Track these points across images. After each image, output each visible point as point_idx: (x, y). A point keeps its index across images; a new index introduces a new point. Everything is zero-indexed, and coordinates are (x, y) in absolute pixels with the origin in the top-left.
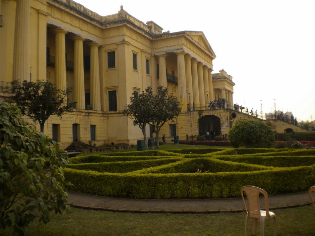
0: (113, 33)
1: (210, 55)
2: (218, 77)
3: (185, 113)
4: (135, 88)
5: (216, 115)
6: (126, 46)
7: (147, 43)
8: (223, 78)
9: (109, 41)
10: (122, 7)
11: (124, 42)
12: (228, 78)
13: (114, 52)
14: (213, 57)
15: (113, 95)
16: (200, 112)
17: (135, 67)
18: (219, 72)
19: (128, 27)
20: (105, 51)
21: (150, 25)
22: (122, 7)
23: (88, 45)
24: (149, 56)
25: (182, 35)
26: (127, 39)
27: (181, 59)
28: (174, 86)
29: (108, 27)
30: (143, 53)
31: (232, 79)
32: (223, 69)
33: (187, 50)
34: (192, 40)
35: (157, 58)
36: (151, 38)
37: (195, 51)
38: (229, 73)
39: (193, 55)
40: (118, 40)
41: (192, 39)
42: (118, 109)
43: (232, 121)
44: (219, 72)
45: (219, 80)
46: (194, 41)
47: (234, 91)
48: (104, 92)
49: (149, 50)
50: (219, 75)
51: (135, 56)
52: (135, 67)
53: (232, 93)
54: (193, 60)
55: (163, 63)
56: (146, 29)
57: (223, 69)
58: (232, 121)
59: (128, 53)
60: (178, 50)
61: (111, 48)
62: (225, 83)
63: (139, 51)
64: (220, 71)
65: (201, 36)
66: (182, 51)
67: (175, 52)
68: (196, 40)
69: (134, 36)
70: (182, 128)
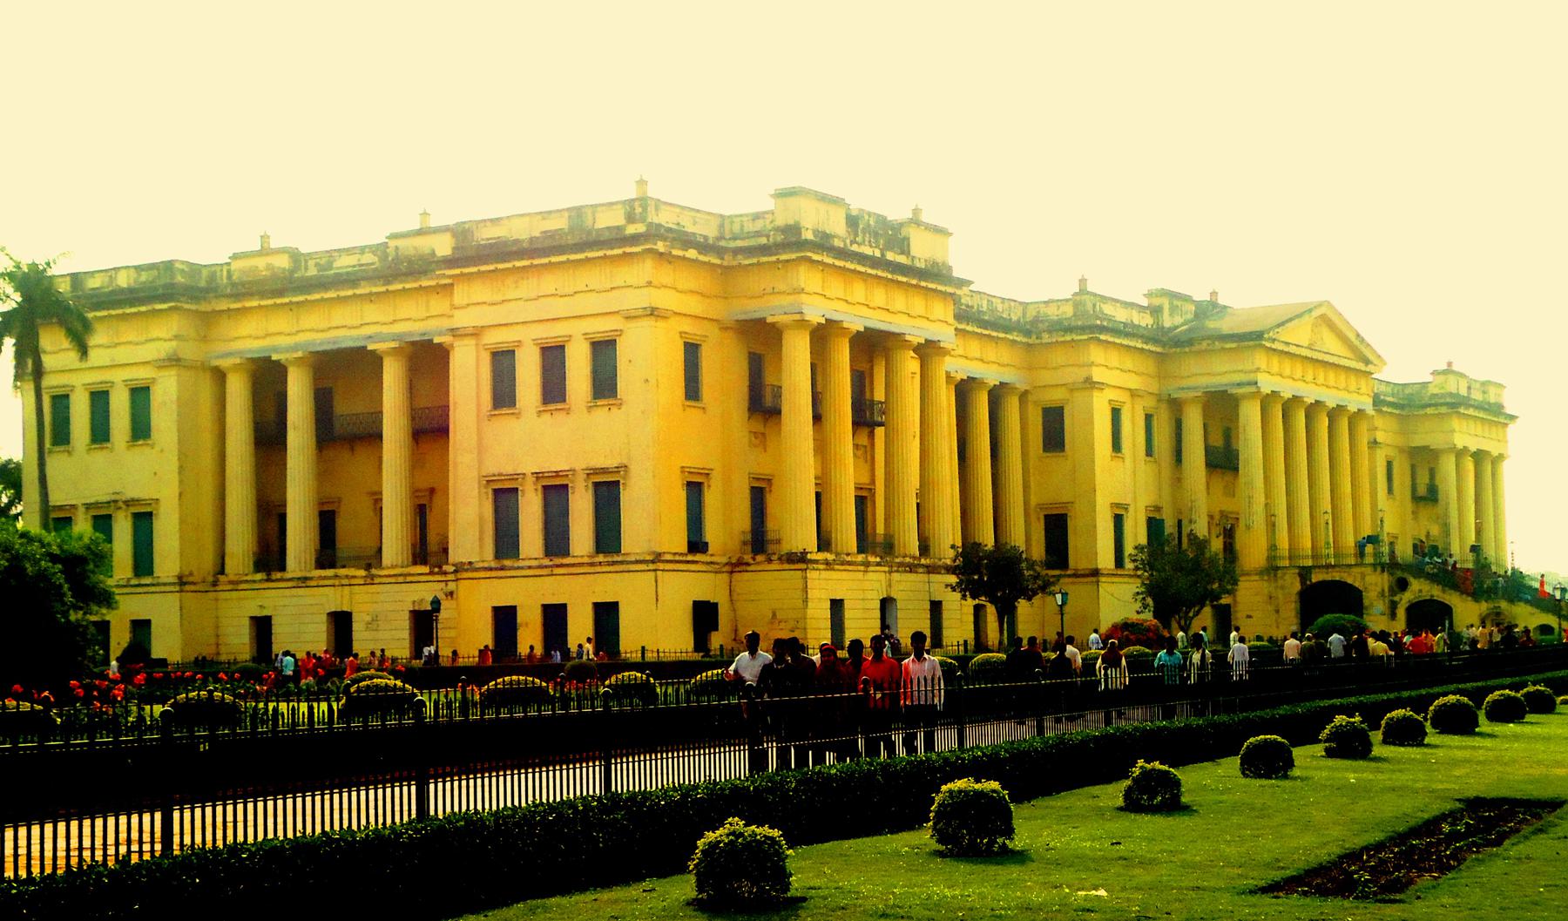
0: (1058, 357)
1: (1361, 359)
2: (1426, 400)
3: (1261, 573)
4: (1117, 505)
5: (1350, 581)
6: (1096, 394)
7: (1149, 366)
8: (1447, 404)
9: (1046, 377)
10: (1083, 281)
11: (1090, 384)
12: (1477, 396)
15: (1057, 527)
16: (1304, 573)
17: (1116, 445)
21: (1156, 302)
22: (1083, 281)
23: (997, 396)
26: (1098, 375)
27: (1250, 414)
28: (1229, 477)
29: (1046, 338)
33: (1267, 384)
34: (1286, 349)
36: (1159, 350)
40: (1076, 375)
41: (1287, 344)
42: (1072, 563)
43: (1396, 598)
44: (1429, 378)
45: (1429, 411)
46: (1293, 349)
48: (1033, 517)
50: (1433, 390)
51: (1116, 414)
53: (1501, 457)
56: (1146, 321)
58: (1396, 598)
61: (1055, 397)
62: (1456, 423)
66: (1253, 389)
68: (1298, 335)
69: (1114, 358)
70: (1249, 617)
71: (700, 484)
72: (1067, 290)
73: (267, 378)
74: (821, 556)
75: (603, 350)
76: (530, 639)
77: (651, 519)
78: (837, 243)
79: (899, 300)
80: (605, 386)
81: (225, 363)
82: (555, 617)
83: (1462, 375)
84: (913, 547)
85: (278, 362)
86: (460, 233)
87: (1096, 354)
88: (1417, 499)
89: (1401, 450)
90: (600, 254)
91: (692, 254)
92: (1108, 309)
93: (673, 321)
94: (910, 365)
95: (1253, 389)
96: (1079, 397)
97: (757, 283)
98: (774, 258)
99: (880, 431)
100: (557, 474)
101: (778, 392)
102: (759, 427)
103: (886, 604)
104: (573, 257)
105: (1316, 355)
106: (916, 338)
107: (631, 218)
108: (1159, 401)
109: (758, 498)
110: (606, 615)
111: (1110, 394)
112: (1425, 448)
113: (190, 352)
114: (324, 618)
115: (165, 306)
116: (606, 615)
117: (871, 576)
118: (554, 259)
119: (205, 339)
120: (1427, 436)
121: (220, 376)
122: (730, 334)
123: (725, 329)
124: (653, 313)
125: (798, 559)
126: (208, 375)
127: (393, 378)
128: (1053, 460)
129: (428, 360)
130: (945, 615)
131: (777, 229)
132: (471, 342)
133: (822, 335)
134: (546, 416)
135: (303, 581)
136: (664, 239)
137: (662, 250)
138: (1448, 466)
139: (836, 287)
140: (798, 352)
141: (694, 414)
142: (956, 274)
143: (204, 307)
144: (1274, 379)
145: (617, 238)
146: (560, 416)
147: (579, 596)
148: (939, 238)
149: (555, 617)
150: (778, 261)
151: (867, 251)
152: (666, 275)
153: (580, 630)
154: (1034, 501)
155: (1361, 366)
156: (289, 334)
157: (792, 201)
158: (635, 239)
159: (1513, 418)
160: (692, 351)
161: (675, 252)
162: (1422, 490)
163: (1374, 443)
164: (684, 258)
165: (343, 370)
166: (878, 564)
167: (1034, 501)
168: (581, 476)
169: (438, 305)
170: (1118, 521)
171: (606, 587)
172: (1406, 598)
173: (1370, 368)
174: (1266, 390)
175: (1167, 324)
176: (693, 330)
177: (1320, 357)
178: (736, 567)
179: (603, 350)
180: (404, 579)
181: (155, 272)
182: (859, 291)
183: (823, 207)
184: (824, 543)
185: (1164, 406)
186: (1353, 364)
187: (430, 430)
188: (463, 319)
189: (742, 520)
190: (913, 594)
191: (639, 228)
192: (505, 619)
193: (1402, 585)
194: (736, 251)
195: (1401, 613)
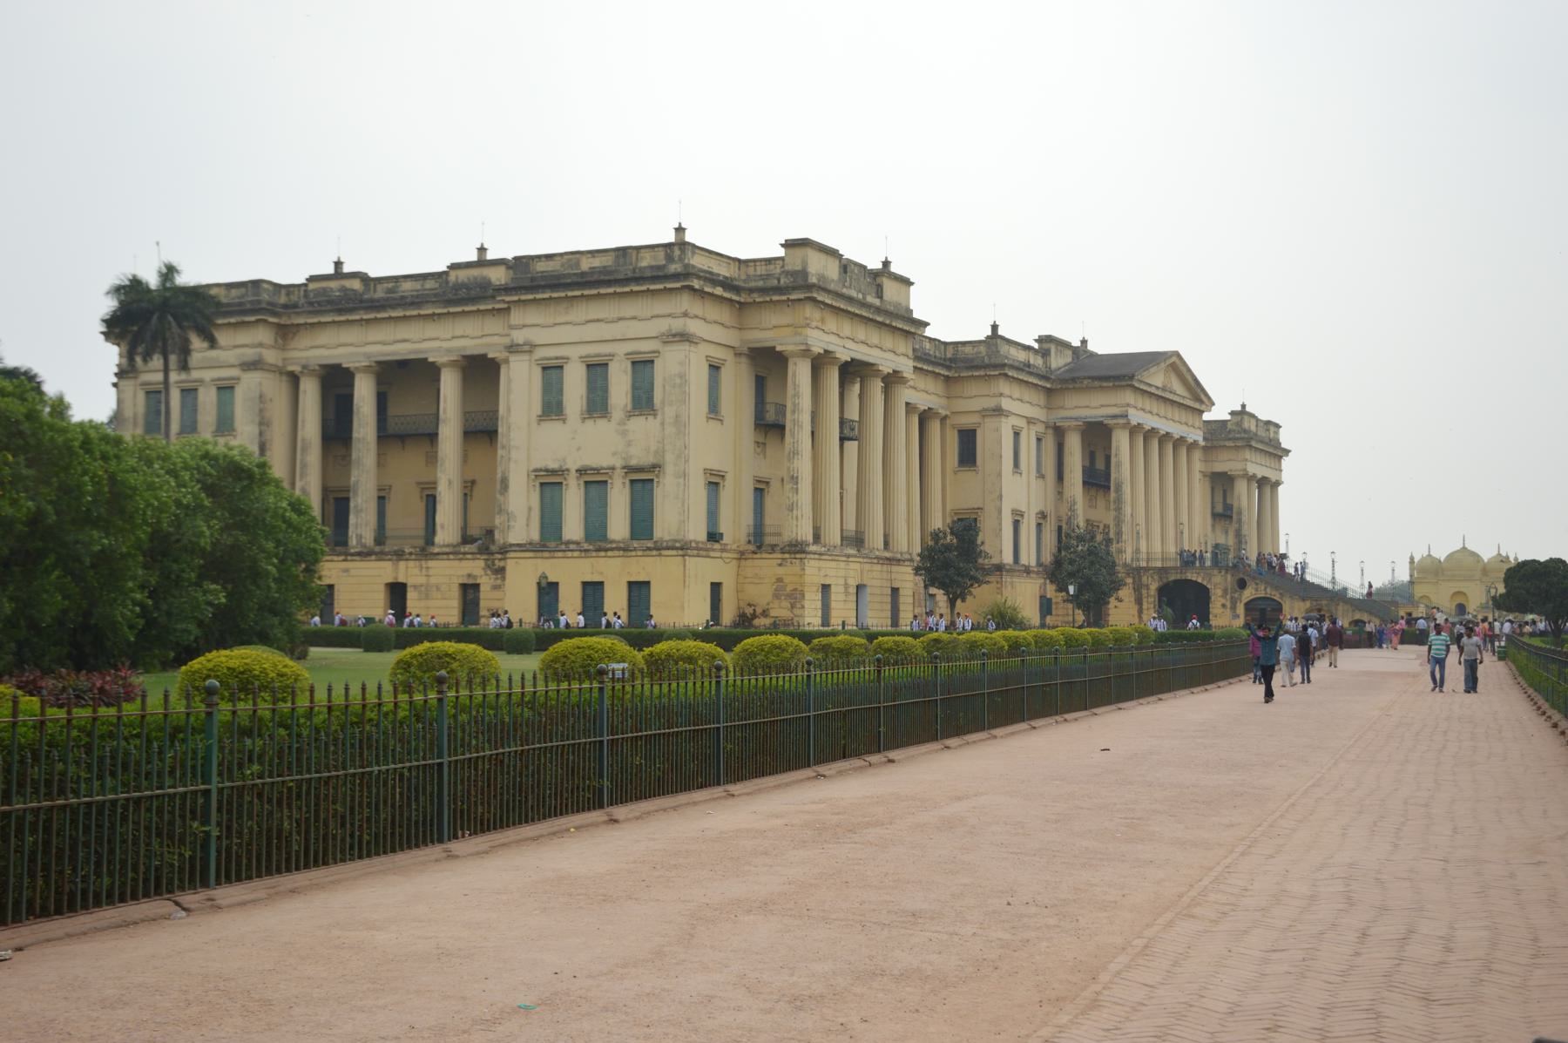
0: (973, 389)
7: (1040, 398)
11: (998, 412)
12: (1262, 433)
13: (974, 431)
14: (1203, 407)
17: (1016, 464)
20: (953, 426)
21: (1046, 346)
22: (995, 327)
23: (925, 418)
24: (1040, 428)
26: (1006, 404)
27: (1121, 440)
31: (1277, 433)
32: (1243, 406)
33: (1135, 417)
35: (1059, 433)
38: (1263, 417)
39: (1150, 422)
46: (1153, 390)
47: (1285, 476)
51: (1017, 434)
52: (1016, 464)
53: (1278, 483)
54: (1150, 434)
55: (1074, 444)
56: (1037, 361)
57: (1243, 406)
60: (1114, 417)
61: (967, 421)
62: (1248, 454)
63: (1021, 423)
64: (1232, 413)
65: (1174, 364)
68: (1156, 378)
69: (1016, 391)
72: (983, 333)
73: (336, 382)
74: (813, 548)
75: (642, 366)
76: (571, 612)
77: (681, 511)
78: (832, 287)
79: (875, 336)
80: (643, 402)
81: (296, 368)
82: (593, 592)
83: (1253, 416)
84: (881, 545)
85: (347, 369)
86: (521, 263)
87: (1004, 387)
88: (1215, 516)
90: (644, 288)
91: (719, 291)
92: (1013, 352)
94: (877, 386)
95: (1122, 421)
96: (990, 423)
99: (851, 447)
100: (597, 471)
101: (781, 409)
102: (761, 440)
104: (619, 290)
106: (886, 368)
107: (670, 259)
109: (760, 492)
110: (639, 591)
111: (1013, 421)
112: (1225, 474)
113: (271, 356)
114: (382, 588)
115: (253, 319)
116: (639, 591)
117: (853, 566)
118: (603, 291)
119: (283, 349)
121: (294, 379)
122: (744, 360)
123: (738, 355)
124: (684, 337)
125: (796, 549)
126: (284, 378)
127: (450, 385)
128: (967, 476)
129: (481, 372)
130: (902, 600)
131: (787, 273)
132: (526, 357)
133: (819, 363)
134: (590, 422)
135: (365, 554)
136: (699, 277)
138: (1241, 487)
139: (832, 323)
140: (801, 373)
141: (714, 424)
142: (915, 316)
143: (284, 320)
144: (1145, 415)
145: (657, 275)
146: (601, 423)
147: (616, 574)
149: (593, 592)
151: (853, 293)
152: (696, 307)
153: (616, 603)
154: (948, 508)
155: (1197, 405)
156: (356, 345)
157: (799, 253)
158: (676, 277)
159: (1287, 452)
162: (1220, 509)
164: (712, 295)
165: (405, 377)
167: (948, 508)
168: (619, 473)
169: (492, 325)
170: (1016, 524)
171: (640, 568)
172: (1249, 594)
173: (1203, 407)
174: (1134, 423)
175: (1054, 366)
176: (718, 353)
177: (1171, 397)
178: (742, 556)
179: (642, 366)
180: (454, 553)
181: (243, 290)
182: (847, 328)
183: (823, 256)
184: (817, 538)
185: (1050, 431)
187: (482, 432)
188: (519, 337)
189: (748, 519)
190: (877, 578)
191: (675, 268)
192: (548, 592)
193: (1242, 584)
194: (751, 291)
195: (1241, 609)
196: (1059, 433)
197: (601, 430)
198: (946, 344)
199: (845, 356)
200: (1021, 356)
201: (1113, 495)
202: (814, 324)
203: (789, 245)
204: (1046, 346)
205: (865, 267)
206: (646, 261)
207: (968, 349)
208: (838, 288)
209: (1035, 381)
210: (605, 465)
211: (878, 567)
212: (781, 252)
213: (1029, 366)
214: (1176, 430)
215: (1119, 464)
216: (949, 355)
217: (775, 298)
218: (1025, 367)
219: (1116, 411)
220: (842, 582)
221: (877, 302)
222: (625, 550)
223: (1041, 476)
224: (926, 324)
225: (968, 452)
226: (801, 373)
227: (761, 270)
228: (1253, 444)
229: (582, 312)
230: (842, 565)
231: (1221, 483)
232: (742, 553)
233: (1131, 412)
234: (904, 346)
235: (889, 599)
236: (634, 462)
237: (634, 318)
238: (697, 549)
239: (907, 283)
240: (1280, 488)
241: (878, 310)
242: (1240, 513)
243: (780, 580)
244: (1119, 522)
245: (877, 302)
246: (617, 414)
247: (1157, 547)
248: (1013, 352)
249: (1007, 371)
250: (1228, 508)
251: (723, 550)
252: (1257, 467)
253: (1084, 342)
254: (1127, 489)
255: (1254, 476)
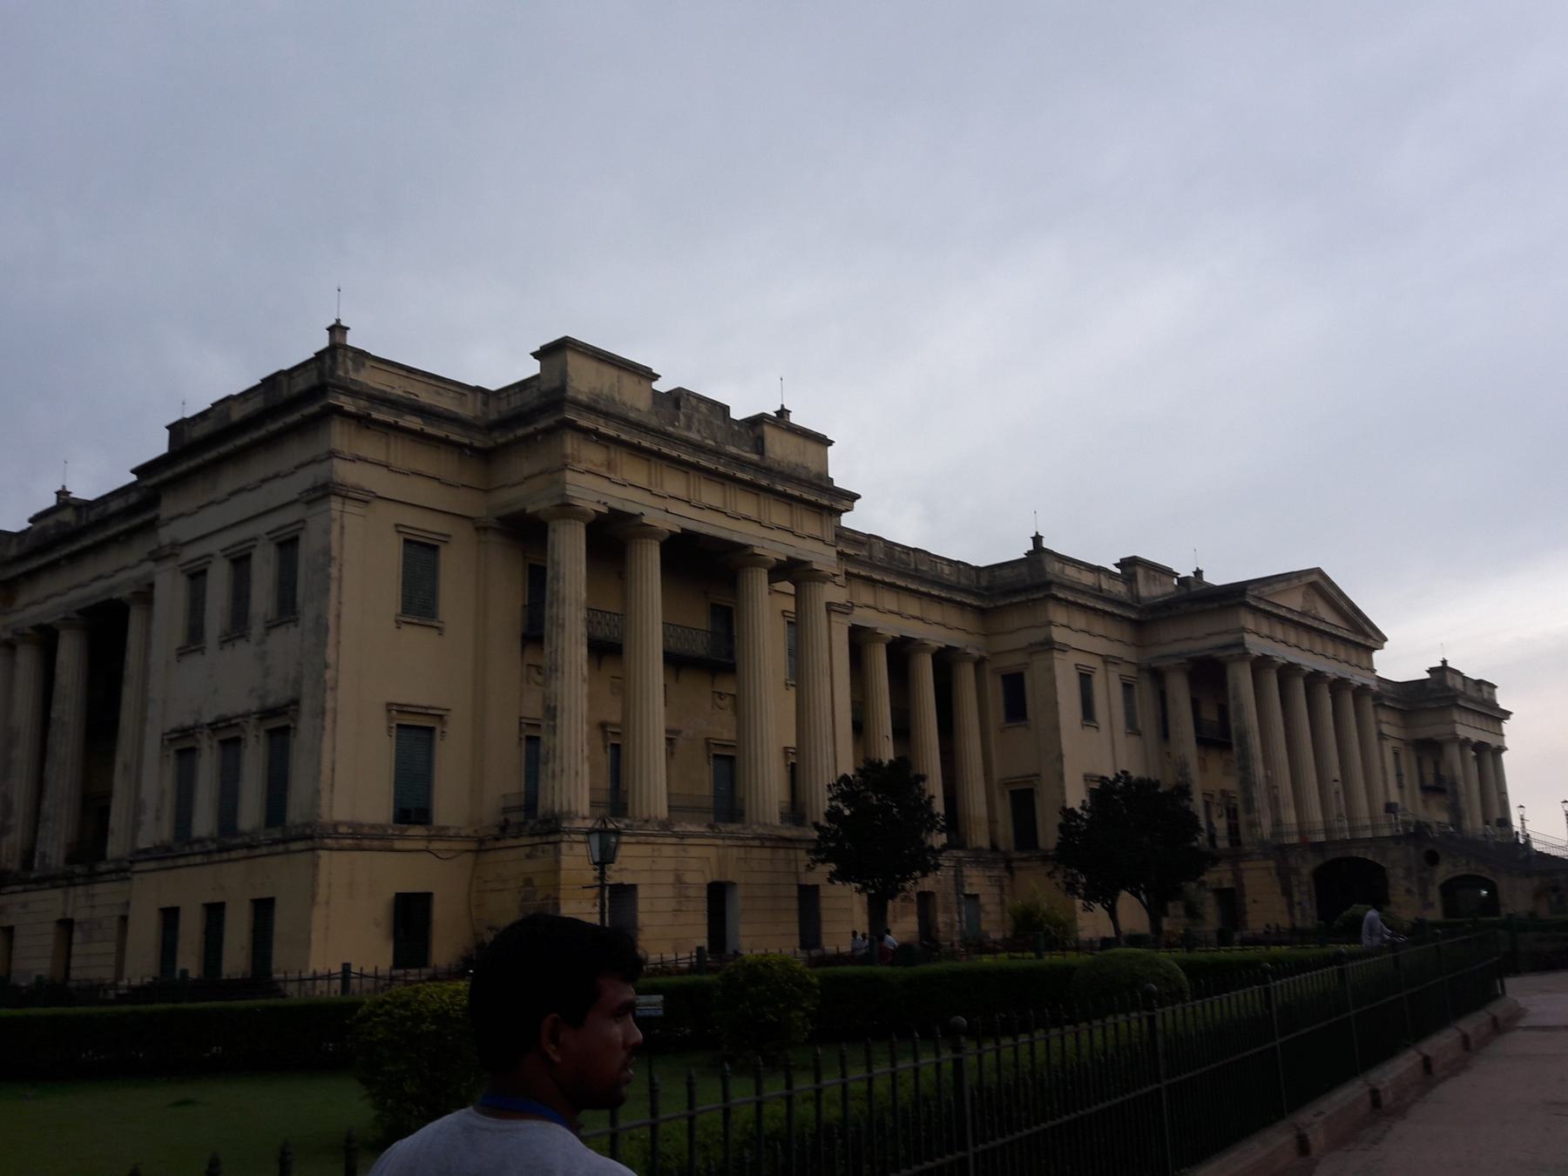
1: (1362, 635)
5: (1370, 858)
6: (1056, 654)
11: (1049, 645)
14: (1370, 643)
18: (1427, 676)
19: (1058, 600)
24: (1129, 671)
25: (1235, 596)
26: (1058, 635)
27: (1242, 679)
30: (1111, 668)
31: (1492, 694)
32: (1444, 662)
33: (1256, 645)
35: (1157, 676)
37: (1292, 638)
38: (1472, 673)
44: (1427, 676)
46: (1283, 613)
47: (1508, 742)
49: (1127, 653)
51: (1085, 679)
53: (1501, 749)
54: (1287, 672)
55: (1179, 689)
56: (1119, 588)
57: (1444, 662)
59: (1065, 672)
62: (1456, 715)
63: (1096, 663)
64: (1431, 671)
65: (1316, 584)
67: (1219, 654)
69: (1080, 621)
71: (431, 730)
79: (746, 504)
88: (1426, 789)
89: (1407, 743)
92: (1071, 571)
93: (379, 506)
95: (1236, 651)
97: (520, 466)
98: (530, 429)
103: (718, 894)
105: (1309, 622)
108: (1140, 670)
117: (694, 852)
120: (1429, 728)
123: (481, 528)
136: (354, 394)
137: (352, 409)
138: (1453, 753)
148: (812, 447)
150: (538, 432)
159: (1507, 714)
160: (421, 554)
161: (375, 415)
163: (1381, 736)
166: (701, 835)
168: (253, 720)
177: (1316, 624)
183: (610, 374)
186: (1352, 637)
196: (1157, 676)
197: (243, 652)
198: (977, 569)
199: (670, 524)
200: (1088, 579)
201: (1235, 749)
202: (582, 467)
203: (542, 354)
204: (1129, 570)
205: (725, 409)
206: (301, 384)
207: (1006, 572)
208: (654, 422)
209: (1109, 608)
210: (240, 710)
211: (767, 853)
212: (533, 368)
213: (1101, 590)
214: (1332, 669)
215: (1240, 709)
216: (984, 583)
217: (520, 432)
218: (1098, 593)
219: (1229, 639)
220: (671, 879)
221: (755, 457)
222: (249, 847)
223: (1132, 728)
224: (856, 497)
225: (1016, 699)
226: (570, 550)
227: (516, 401)
228: (1461, 703)
229: (229, 480)
230: (668, 851)
231: (1429, 748)
232: (481, 841)
233: (1250, 640)
234: (810, 525)
235: (794, 905)
236: (271, 701)
237: (276, 476)
238: (352, 836)
239: (825, 442)
240: (1505, 755)
241: (756, 467)
242: (1454, 783)
243: (528, 882)
244: (1246, 783)
245: (755, 457)
246: (257, 629)
247: (1316, 815)
248: (1071, 571)
249: (1054, 591)
250: (1439, 777)
251: (429, 838)
252: (1469, 730)
253: (1198, 573)
254: (1255, 741)
255: (1467, 740)
